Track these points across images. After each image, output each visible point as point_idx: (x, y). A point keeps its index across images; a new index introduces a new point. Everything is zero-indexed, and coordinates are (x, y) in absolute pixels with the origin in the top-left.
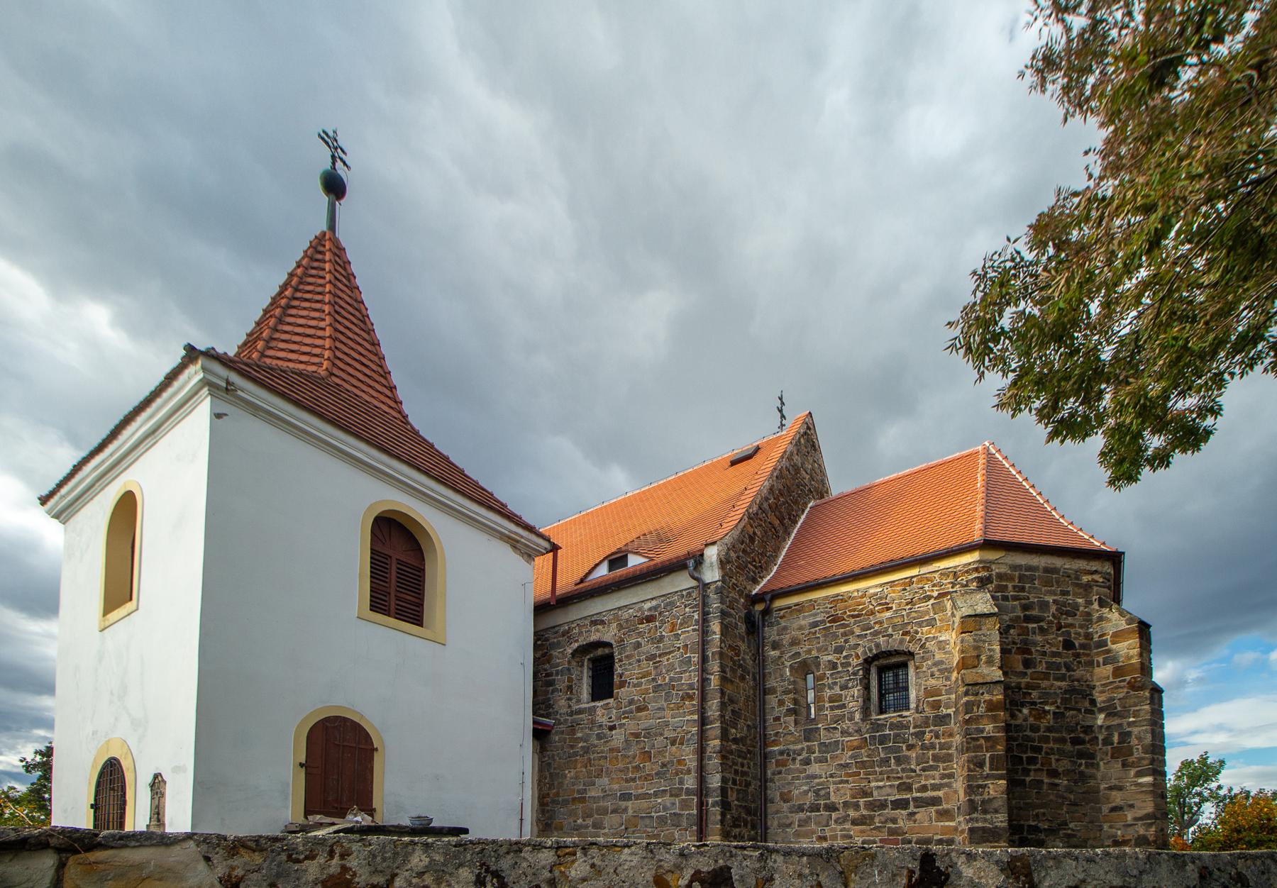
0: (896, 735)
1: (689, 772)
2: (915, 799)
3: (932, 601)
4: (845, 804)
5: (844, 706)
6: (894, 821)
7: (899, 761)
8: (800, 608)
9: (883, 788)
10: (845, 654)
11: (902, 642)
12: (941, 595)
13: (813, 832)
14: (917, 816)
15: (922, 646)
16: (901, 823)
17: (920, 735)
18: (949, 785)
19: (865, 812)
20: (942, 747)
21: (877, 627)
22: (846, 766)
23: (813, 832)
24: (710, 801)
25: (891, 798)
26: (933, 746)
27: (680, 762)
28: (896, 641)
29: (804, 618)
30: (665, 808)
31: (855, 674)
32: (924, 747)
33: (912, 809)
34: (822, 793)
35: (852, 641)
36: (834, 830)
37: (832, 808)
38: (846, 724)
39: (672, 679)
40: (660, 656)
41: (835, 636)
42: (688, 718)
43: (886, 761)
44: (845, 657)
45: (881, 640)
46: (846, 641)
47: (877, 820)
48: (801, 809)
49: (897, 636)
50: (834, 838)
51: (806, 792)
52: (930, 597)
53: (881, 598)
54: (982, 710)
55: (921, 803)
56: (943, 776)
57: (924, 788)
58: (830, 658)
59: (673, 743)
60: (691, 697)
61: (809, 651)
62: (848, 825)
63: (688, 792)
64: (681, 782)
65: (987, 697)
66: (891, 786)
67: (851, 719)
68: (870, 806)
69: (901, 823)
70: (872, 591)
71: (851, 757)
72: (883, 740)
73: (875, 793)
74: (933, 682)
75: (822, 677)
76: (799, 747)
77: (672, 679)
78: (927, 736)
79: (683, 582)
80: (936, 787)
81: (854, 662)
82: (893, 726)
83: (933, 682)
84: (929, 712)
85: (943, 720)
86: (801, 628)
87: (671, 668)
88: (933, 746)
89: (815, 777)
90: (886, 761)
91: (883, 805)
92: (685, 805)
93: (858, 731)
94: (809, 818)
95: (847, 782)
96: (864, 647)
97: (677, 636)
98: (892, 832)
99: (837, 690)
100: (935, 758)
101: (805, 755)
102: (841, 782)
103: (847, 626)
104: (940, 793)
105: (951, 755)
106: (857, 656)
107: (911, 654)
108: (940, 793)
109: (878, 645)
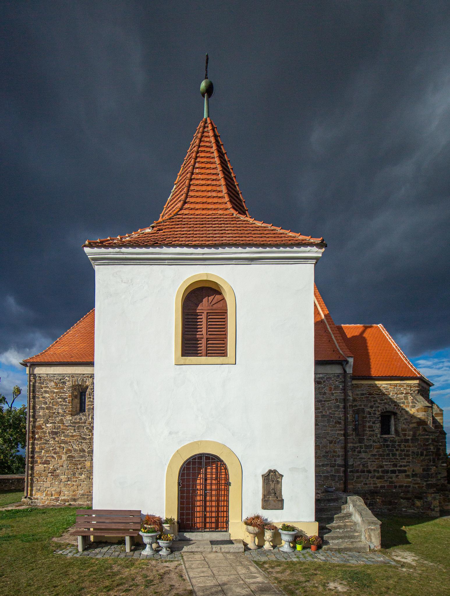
0: (393, 445)
1: (339, 456)
2: (398, 470)
3: (404, 395)
4: (375, 471)
5: (374, 431)
6: (391, 478)
8: (357, 386)
9: (387, 465)
10: (374, 409)
11: (394, 408)
12: (406, 393)
13: (362, 481)
14: (399, 477)
15: (401, 412)
16: (394, 479)
17: (399, 446)
18: (409, 465)
19: (381, 474)
20: (408, 451)
21: (386, 401)
22: (374, 455)
23: (362, 481)
24: (349, 470)
25: (390, 469)
26: (404, 450)
27: (334, 452)
29: (359, 390)
30: (328, 472)
31: (378, 418)
32: (401, 451)
33: (397, 474)
34: (366, 465)
35: (377, 405)
36: (370, 481)
37: (369, 472)
39: (330, 413)
40: (324, 401)
41: (371, 402)
42: (339, 432)
43: (388, 455)
44: (374, 410)
45: (387, 406)
46: (375, 404)
47: (385, 477)
48: (357, 471)
49: (393, 406)
50: (370, 484)
51: (359, 465)
53: (387, 389)
54: (430, 441)
55: (400, 472)
56: (407, 462)
57: (401, 466)
58: (368, 410)
59: (331, 442)
60: (340, 423)
63: (339, 466)
64: (335, 461)
65: (431, 437)
66: (390, 464)
67: (376, 436)
68: (383, 472)
69: (394, 479)
70: (384, 386)
71: (377, 452)
72: (388, 446)
73: (385, 467)
74: (404, 426)
75: (366, 417)
76: (357, 445)
77: (330, 413)
78: (402, 446)
79: (337, 370)
80: (405, 466)
81: (378, 413)
82: (391, 441)
83: (404, 426)
84: (403, 437)
85: (407, 441)
86: (357, 395)
87: (330, 408)
88: (404, 450)
91: (387, 472)
92: (337, 471)
93: (379, 441)
94: (361, 476)
95: (375, 462)
97: (333, 394)
98: (391, 482)
99: (371, 424)
100: (405, 455)
101: (359, 449)
102: (373, 461)
103: (374, 398)
104: (406, 468)
105: (410, 454)
106: (379, 411)
107: (395, 414)
108: (406, 468)
109: (386, 408)
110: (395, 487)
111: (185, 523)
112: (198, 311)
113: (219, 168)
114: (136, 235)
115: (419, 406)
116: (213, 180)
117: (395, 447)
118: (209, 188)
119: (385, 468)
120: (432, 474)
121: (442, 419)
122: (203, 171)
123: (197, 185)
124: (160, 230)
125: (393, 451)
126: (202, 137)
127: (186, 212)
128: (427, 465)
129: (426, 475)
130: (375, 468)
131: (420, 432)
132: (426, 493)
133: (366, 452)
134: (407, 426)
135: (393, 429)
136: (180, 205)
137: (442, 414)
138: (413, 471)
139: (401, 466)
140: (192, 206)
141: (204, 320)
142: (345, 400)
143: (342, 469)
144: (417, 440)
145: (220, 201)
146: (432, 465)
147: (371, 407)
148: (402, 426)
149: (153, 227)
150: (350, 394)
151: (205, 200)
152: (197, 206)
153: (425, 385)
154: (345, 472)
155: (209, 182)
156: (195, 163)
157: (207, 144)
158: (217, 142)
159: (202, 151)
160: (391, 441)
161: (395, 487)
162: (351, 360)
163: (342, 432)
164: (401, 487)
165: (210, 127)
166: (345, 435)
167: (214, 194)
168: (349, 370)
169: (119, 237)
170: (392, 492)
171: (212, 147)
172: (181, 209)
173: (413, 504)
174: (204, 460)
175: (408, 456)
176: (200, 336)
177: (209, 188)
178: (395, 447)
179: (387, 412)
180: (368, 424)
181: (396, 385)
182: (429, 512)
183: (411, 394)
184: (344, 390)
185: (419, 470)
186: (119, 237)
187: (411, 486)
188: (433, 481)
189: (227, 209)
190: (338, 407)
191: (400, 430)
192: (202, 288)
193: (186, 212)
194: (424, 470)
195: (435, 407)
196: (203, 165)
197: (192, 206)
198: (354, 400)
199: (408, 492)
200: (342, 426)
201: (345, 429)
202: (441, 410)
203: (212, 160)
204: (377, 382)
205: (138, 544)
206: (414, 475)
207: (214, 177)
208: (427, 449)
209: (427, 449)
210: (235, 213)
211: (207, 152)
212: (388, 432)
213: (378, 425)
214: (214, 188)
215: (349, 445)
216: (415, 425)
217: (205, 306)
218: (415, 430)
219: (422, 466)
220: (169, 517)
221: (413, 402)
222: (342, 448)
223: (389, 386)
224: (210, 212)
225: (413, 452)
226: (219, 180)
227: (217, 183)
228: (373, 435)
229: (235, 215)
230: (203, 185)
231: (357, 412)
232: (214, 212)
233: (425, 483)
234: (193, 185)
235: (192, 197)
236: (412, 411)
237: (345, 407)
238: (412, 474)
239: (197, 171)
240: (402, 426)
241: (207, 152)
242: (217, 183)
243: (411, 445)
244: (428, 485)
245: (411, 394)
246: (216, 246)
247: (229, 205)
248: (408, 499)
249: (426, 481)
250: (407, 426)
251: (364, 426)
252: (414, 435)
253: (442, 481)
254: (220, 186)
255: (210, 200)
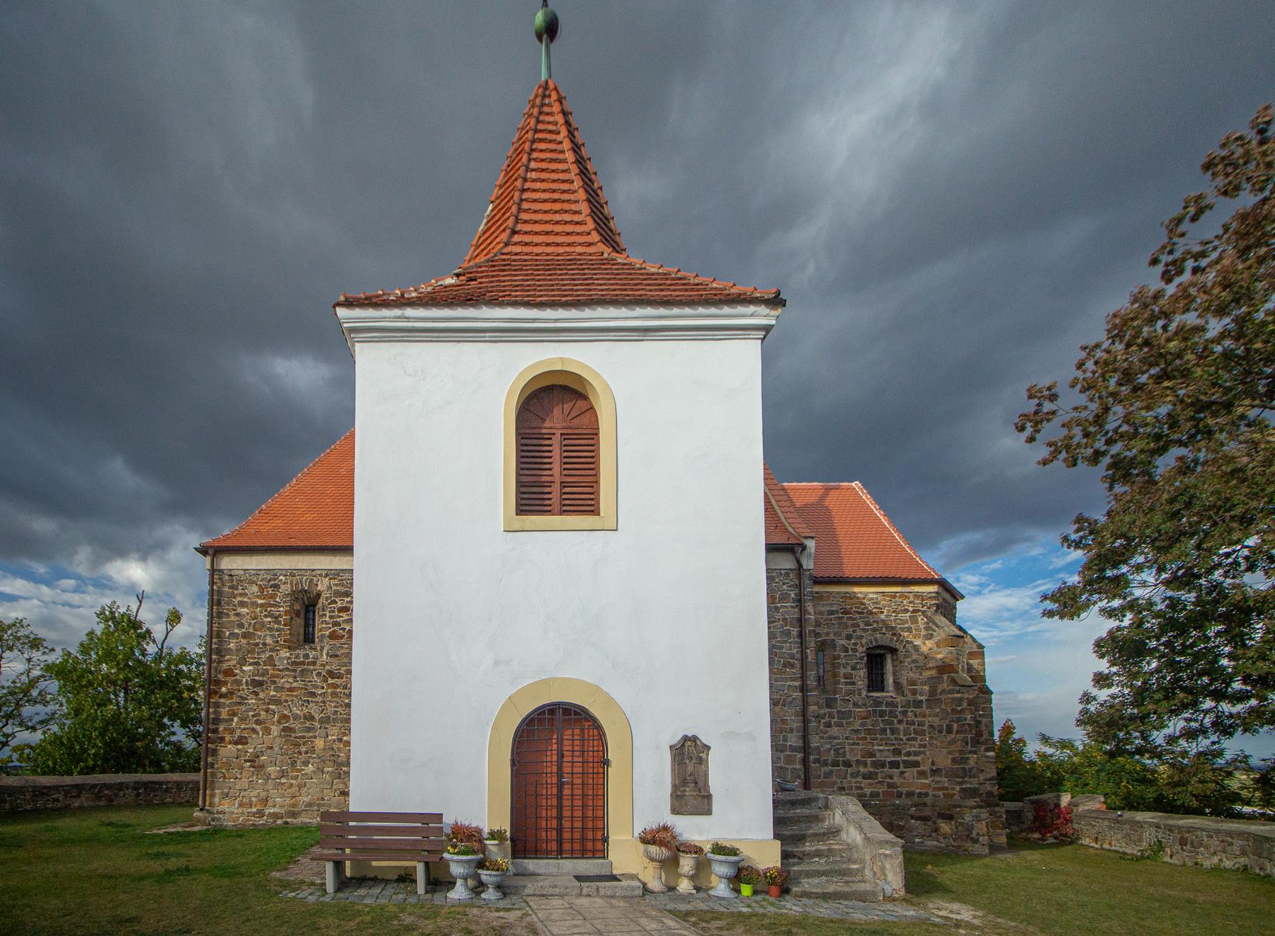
0: (891, 712)
1: (791, 730)
2: (904, 762)
6: (891, 777)
7: (893, 731)
9: (883, 751)
16: (896, 779)
17: (904, 713)
18: (924, 753)
22: (857, 731)
26: (913, 723)
28: (885, 639)
31: (861, 659)
32: (908, 723)
35: (859, 633)
36: (850, 782)
37: (847, 764)
38: (856, 698)
41: (846, 626)
43: (884, 731)
48: (825, 763)
49: (889, 635)
51: (829, 750)
52: (907, 611)
54: (965, 704)
56: (921, 746)
57: (908, 754)
60: (792, 666)
61: (828, 634)
62: (860, 779)
63: (793, 749)
64: (785, 739)
68: (875, 764)
69: (896, 779)
71: (862, 725)
72: (882, 714)
80: (917, 754)
82: (888, 704)
83: (911, 674)
84: (910, 697)
85: (918, 704)
86: (821, 613)
88: (913, 723)
89: (835, 738)
90: (884, 731)
91: (883, 765)
96: (867, 639)
98: (890, 786)
99: (849, 670)
100: (916, 732)
101: (827, 719)
104: (919, 758)
107: (894, 651)
108: (919, 758)
109: (876, 640)
110: (899, 795)
111: (523, 842)
112: (544, 431)
113: (574, 169)
114: (429, 289)
115: (940, 635)
116: (564, 192)
117: (896, 717)
118: (557, 206)
119: (879, 757)
120: (971, 769)
121: (983, 664)
122: (544, 175)
123: (535, 201)
124: (472, 280)
125: (892, 723)
126: (540, 113)
127: (517, 249)
128: (961, 752)
129: (961, 771)
130: (859, 757)
131: (945, 685)
132: (960, 806)
133: (840, 725)
134: (917, 676)
135: (890, 680)
136: (504, 236)
137: (983, 654)
138: (933, 763)
139: (908, 754)
140: (527, 239)
141: (556, 450)
142: (801, 621)
143: (800, 755)
144: (939, 700)
145: (578, 229)
146: (970, 752)
147: (849, 637)
148: (906, 675)
149: (458, 275)
150: (810, 609)
151: (549, 228)
152: (536, 239)
153: (948, 597)
154: (805, 761)
155: (556, 196)
156: (530, 160)
157: (551, 127)
158: (567, 123)
159: (541, 140)
160: (888, 704)
161: (899, 795)
162: (811, 544)
163: (797, 684)
164: (910, 794)
165: (554, 96)
166: (803, 689)
167: (567, 217)
168: (808, 564)
169: (398, 292)
170: (894, 805)
171: (559, 133)
172: (506, 245)
173: (936, 830)
174: (559, 714)
175: (922, 733)
176: (548, 479)
177: (557, 206)
178: (896, 717)
179: (879, 647)
180: (842, 671)
181: (893, 595)
182: (968, 845)
183: (923, 612)
184: (799, 601)
185: (944, 761)
186: (398, 292)
187: (931, 793)
188: (972, 783)
189: (590, 244)
190: (788, 633)
191: (904, 682)
192: (551, 388)
193: (517, 249)
194: (954, 760)
195: (967, 639)
196: (544, 165)
197: (527, 239)
198: (818, 624)
199: (925, 804)
200: (797, 671)
201: (803, 677)
202: (981, 647)
203: (561, 156)
204: (856, 589)
205: (439, 881)
206: (936, 772)
207: (565, 187)
208: (959, 720)
209: (959, 720)
210: (607, 251)
211: (550, 141)
212: (882, 689)
213: (863, 672)
214: (566, 206)
215: (812, 708)
216: (933, 673)
217: (556, 421)
218: (933, 683)
219: (950, 753)
220: (496, 828)
221: (927, 628)
222: (796, 714)
223: (880, 597)
224: (561, 250)
225: (931, 726)
226: (575, 192)
227: (572, 197)
228: (852, 693)
229: (606, 255)
230: (545, 201)
231: (822, 647)
232: (568, 249)
233: (958, 788)
234: (526, 200)
235: (526, 222)
236: (926, 646)
237: (801, 635)
238: (932, 770)
239: (534, 175)
240: (906, 675)
241: (550, 141)
242: (572, 197)
243: (927, 712)
244: (964, 790)
245: (923, 612)
246: (577, 304)
247: (595, 237)
248: (925, 819)
249: (960, 783)
250: (917, 676)
251: (835, 675)
252: (933, 692)
253: (989, 788)
254: (577, 202)
255: (559, 228)
